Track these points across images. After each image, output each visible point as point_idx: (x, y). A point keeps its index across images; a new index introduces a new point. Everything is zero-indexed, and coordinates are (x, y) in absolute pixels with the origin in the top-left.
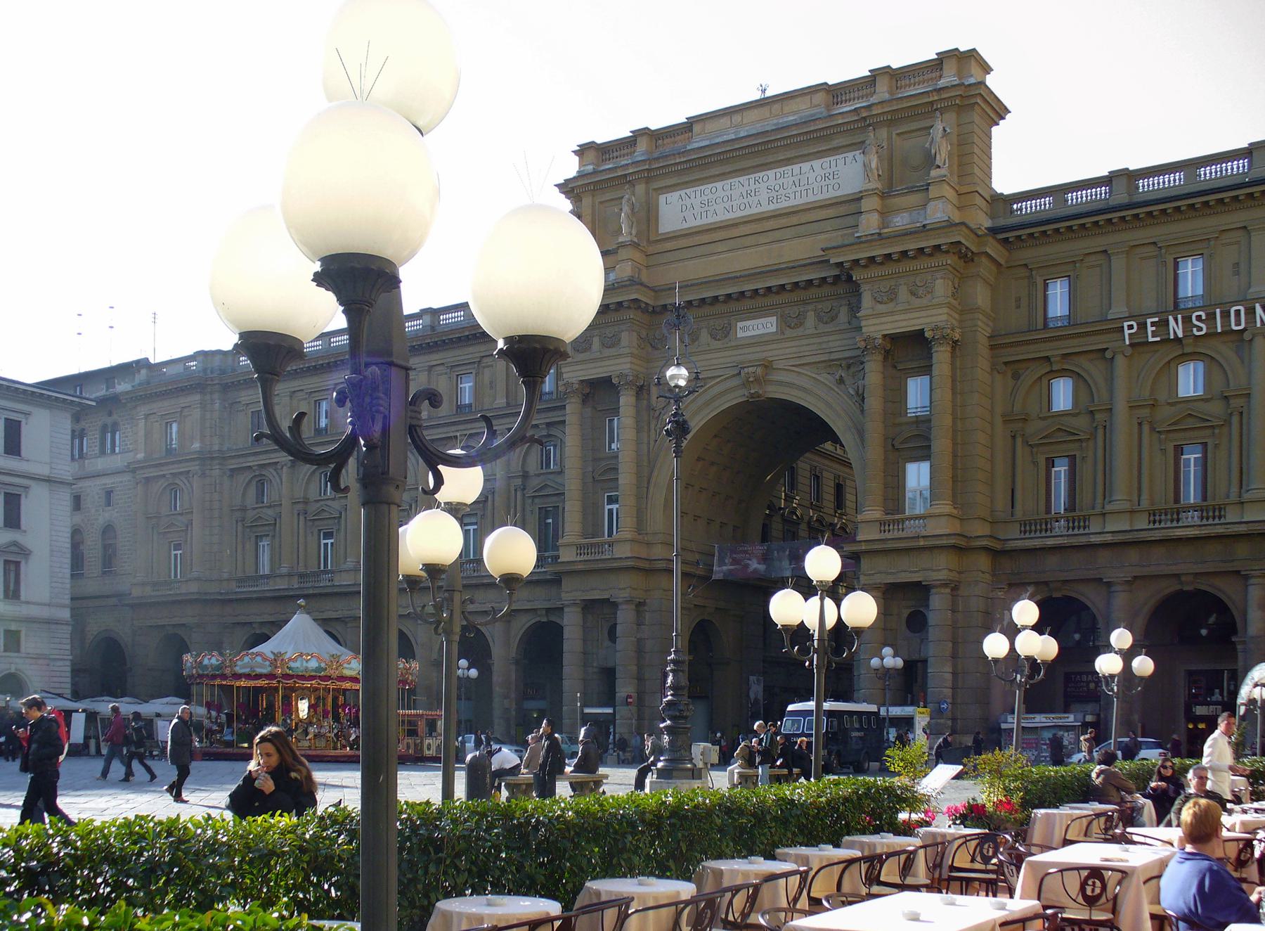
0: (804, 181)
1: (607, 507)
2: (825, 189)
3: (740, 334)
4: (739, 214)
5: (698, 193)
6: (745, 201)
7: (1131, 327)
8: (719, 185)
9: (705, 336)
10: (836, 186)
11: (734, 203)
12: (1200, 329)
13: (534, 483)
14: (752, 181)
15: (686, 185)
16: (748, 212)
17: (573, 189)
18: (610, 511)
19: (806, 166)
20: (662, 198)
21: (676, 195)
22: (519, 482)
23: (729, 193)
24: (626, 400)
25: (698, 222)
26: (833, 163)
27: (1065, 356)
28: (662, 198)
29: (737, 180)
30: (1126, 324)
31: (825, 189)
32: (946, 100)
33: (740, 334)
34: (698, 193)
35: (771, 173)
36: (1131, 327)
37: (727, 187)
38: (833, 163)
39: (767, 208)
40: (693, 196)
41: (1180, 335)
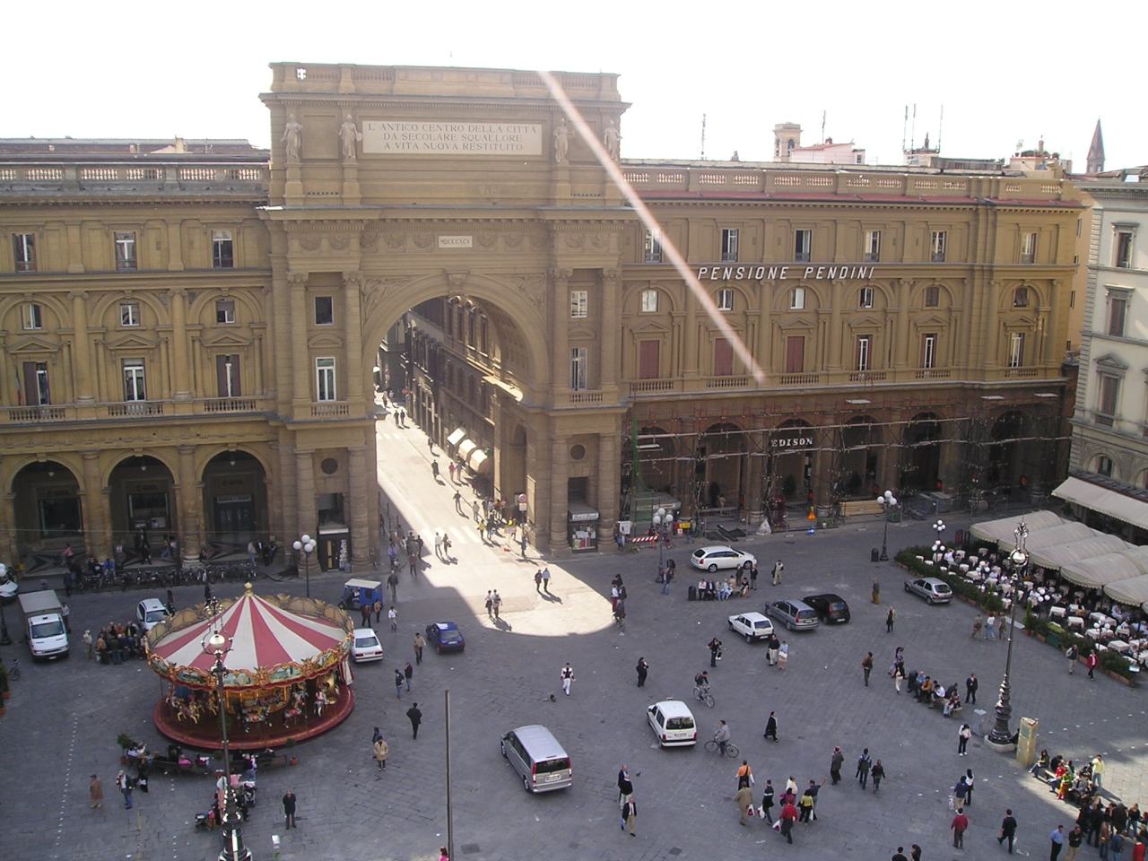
0: (493, 138)
1: (318, 369)
2: (510, 147)
3: (441, 245)
4: (437, 151)
5: (400, 127)
6: (444, 142)
7: (703, 271)
8: (420, 124)
9: (410, 243)
10: (519, 147)
11: (434, 142)
12: (739, 276)
13: (210, 335)
14: (449, 128)
15: (390, 118)
16: (445, 151)
17: (280, 101)
18: (321, 372)
19: (495, 126)
20: (365, 124)
21: (380, 123)
22: (198, 334)
23: (428, 133)
24: (352, 294)
25: (400, 151)
26: (517, 130)
27: (658, 281)
28: (365, 124)
29: (435, 124)
30: (701, 269)
31: (510, 147)
32: (600, 99)
33: (441, 245)
34: (400, 127)
35: (466, 125)
36: (703, 271)
37: (427, 128)
38: (517, 130)
39: (461, 151)
40: (395, 128)
41: (728, 278)
